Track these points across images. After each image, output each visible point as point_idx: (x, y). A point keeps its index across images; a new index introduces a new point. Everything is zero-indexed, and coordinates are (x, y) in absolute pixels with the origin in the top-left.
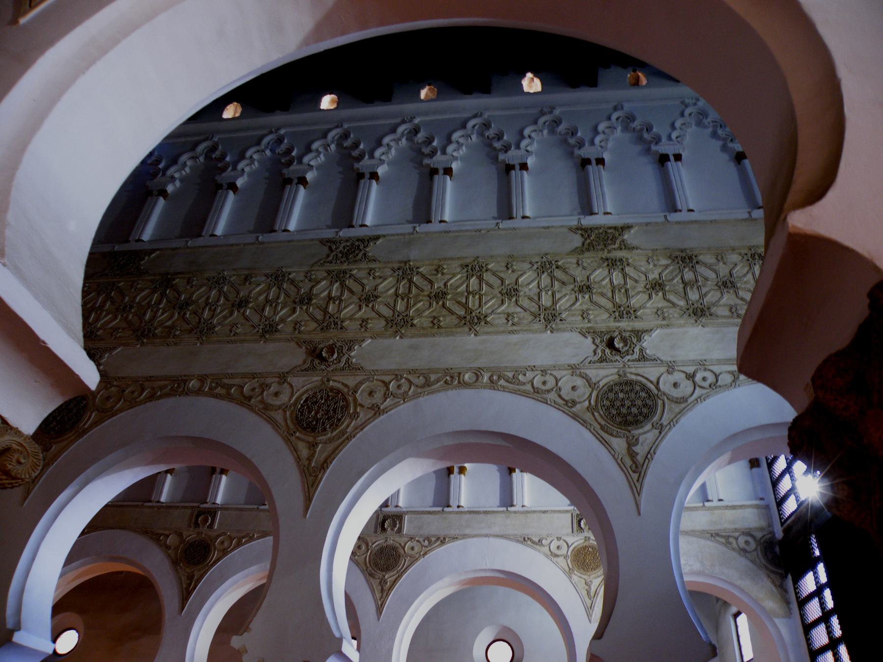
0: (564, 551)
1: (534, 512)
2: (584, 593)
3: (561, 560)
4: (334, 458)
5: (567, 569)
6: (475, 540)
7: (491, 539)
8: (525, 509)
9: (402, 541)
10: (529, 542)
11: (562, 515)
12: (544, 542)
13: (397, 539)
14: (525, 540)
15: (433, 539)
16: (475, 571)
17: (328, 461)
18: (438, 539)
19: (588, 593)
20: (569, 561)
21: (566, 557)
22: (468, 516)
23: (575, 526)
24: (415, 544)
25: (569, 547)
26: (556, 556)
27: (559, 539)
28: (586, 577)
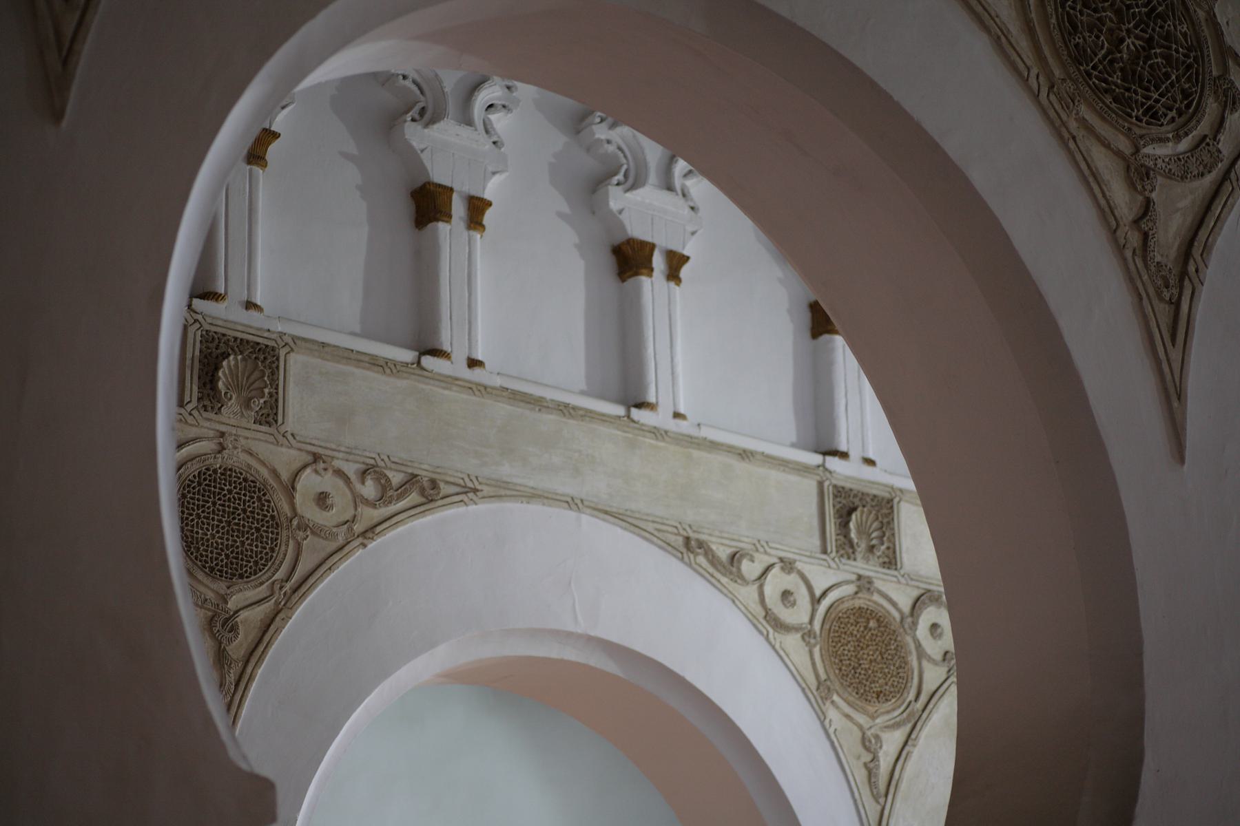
0: (799, 614)
1: (714, 446)
2: (860, 775)
3: (792, 642)
4: (1207, 248)
5: (813, 682)
6: (535, 508)
7: (587, 521)
8: (683, 427)
9: (284, 458)
10: (701, 560)
11: (793, 478)
12: (746, 566)
13: (262, 449)
14: (691, 547)
15: (396, 478)
16: (536, 634)
17: (1196, 252)
18: (412, 479)
19: (871, 773)
20: (817, 650)
21: (807, 635)
22: (502, 410)
23: (831, 528)
24: (327, 482)
25: (816, 601)
26: (780, 626)
27: (788, 566)
28: (862, 719)
